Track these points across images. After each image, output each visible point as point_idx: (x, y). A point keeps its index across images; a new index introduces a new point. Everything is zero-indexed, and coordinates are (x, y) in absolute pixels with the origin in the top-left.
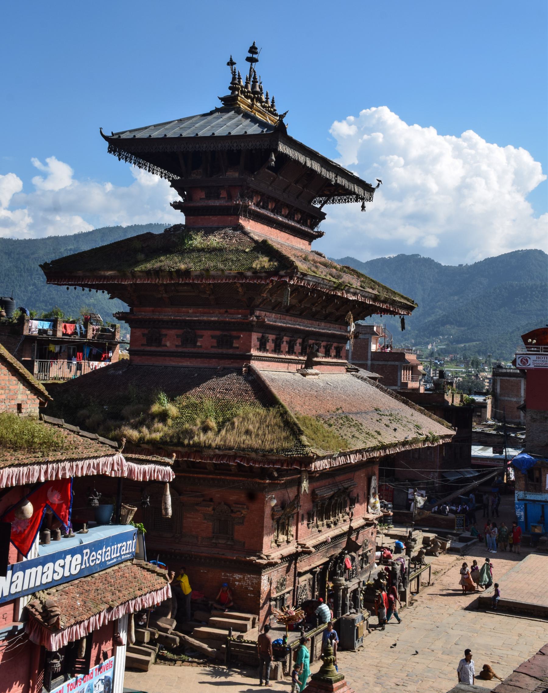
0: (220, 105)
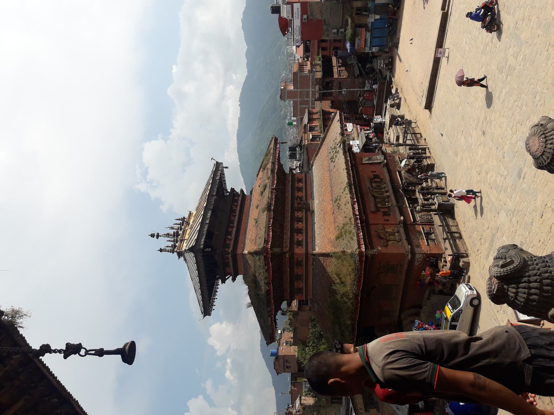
0: (182, 258)
